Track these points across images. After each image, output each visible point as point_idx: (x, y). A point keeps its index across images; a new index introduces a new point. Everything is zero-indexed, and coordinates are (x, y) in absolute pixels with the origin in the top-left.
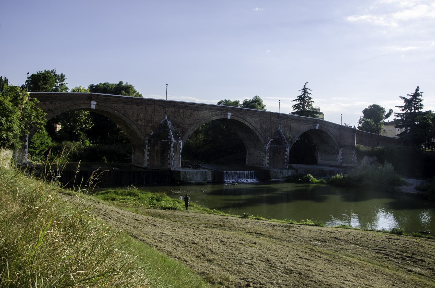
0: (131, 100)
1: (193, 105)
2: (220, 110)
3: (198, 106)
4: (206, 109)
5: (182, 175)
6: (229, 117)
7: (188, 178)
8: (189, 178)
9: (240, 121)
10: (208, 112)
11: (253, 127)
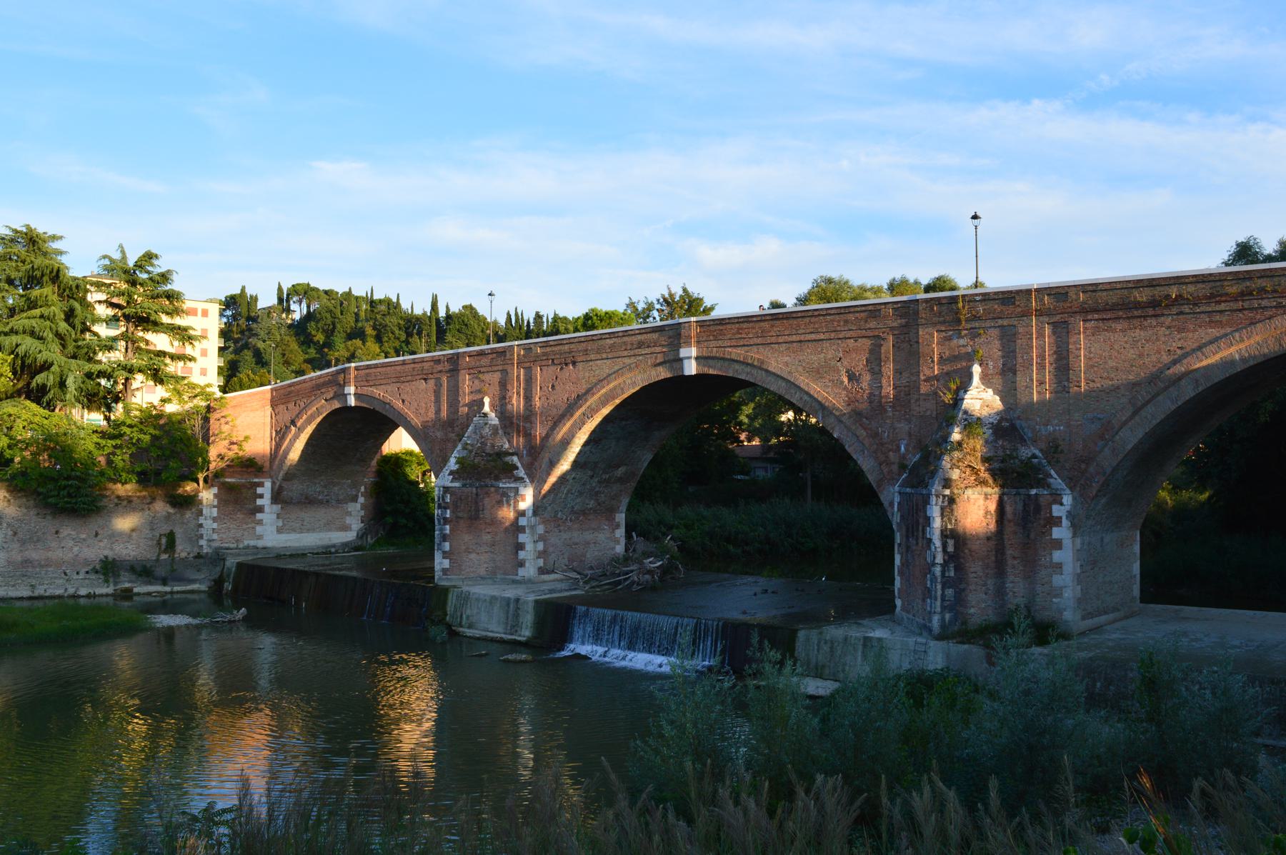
0: (412, 365)
1: (559, 347)
2: (648, 347)
3: (572, 346)
4: (598, 351)
5: (449, 604)
6: (691, 368)
7: (464, 616)
8: (468, 617)
9: (743, 378)
10: (608, 362)
11: (806, 397)
